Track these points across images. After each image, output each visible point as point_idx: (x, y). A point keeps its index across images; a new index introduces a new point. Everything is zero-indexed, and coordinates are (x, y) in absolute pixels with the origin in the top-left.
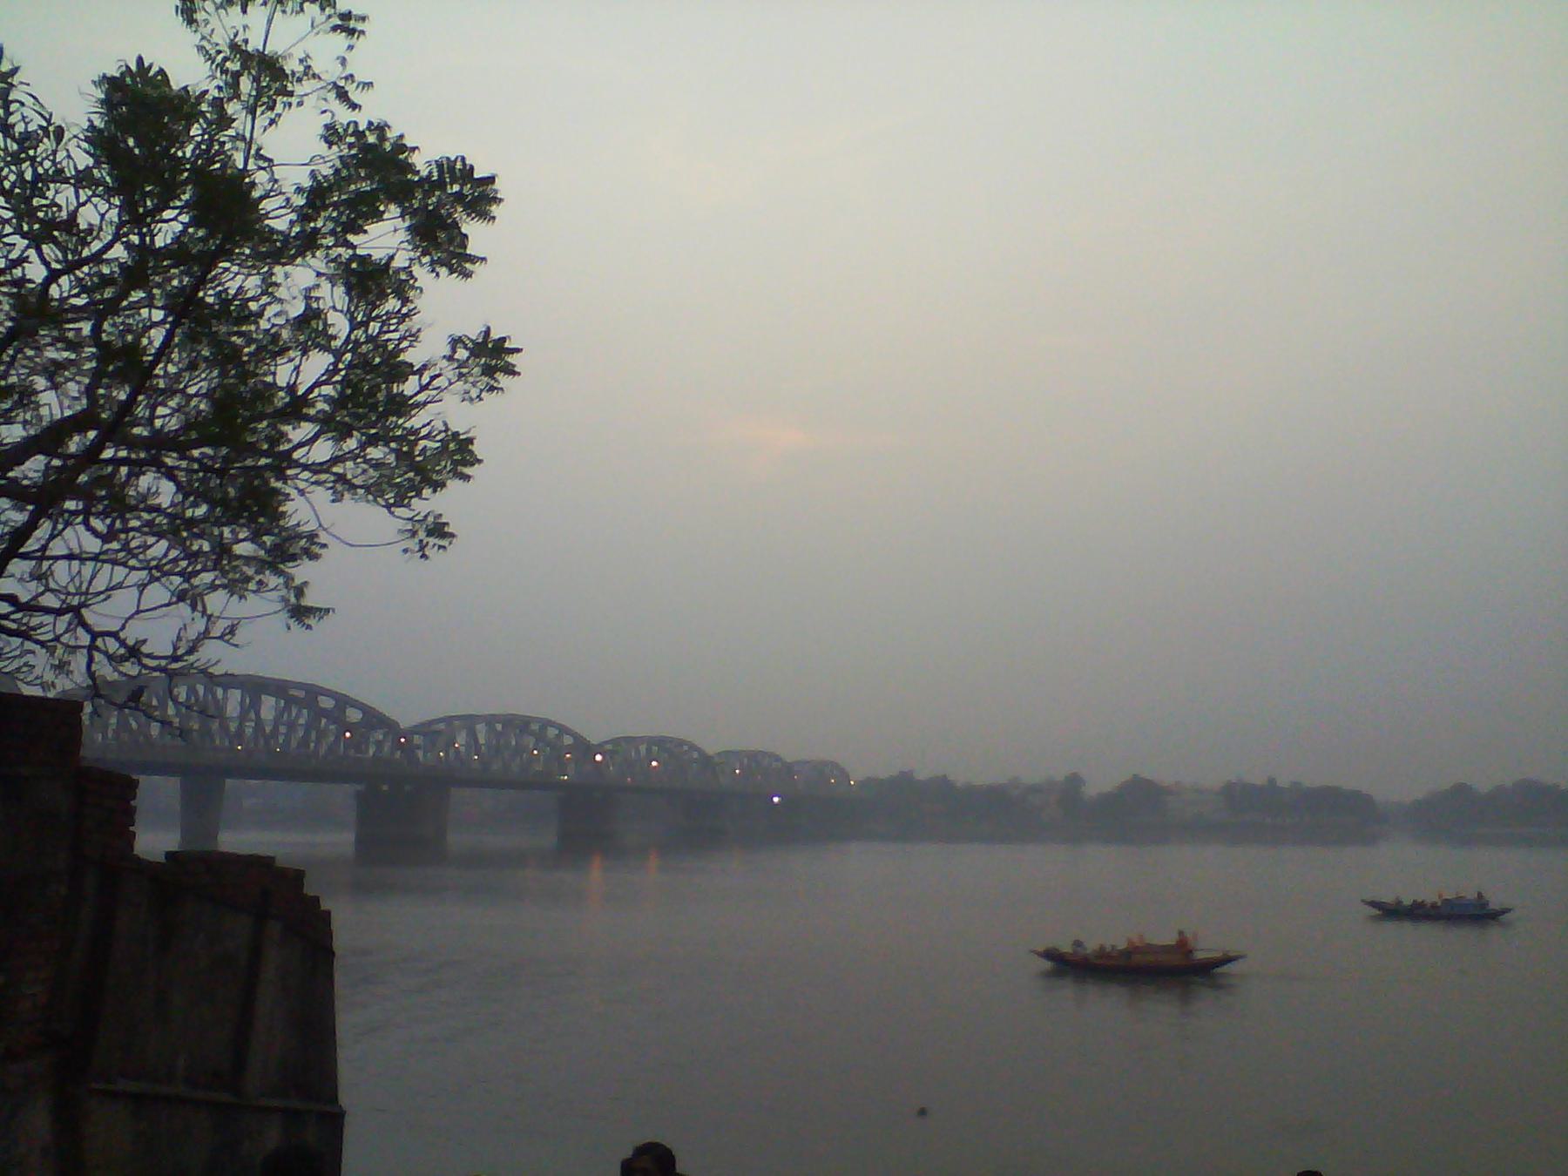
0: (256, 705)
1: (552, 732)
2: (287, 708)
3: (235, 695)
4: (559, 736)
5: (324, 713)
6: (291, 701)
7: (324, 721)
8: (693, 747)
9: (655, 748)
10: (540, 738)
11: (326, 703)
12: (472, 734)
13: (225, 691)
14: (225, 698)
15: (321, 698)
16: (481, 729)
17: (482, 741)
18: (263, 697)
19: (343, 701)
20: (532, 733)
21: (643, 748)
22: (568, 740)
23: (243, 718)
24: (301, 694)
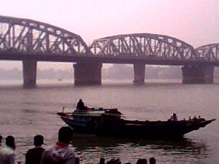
5: (169, 44)
11: (170, 41)
14: (141, 41)
19: (175, 40)
24: (162, 38)
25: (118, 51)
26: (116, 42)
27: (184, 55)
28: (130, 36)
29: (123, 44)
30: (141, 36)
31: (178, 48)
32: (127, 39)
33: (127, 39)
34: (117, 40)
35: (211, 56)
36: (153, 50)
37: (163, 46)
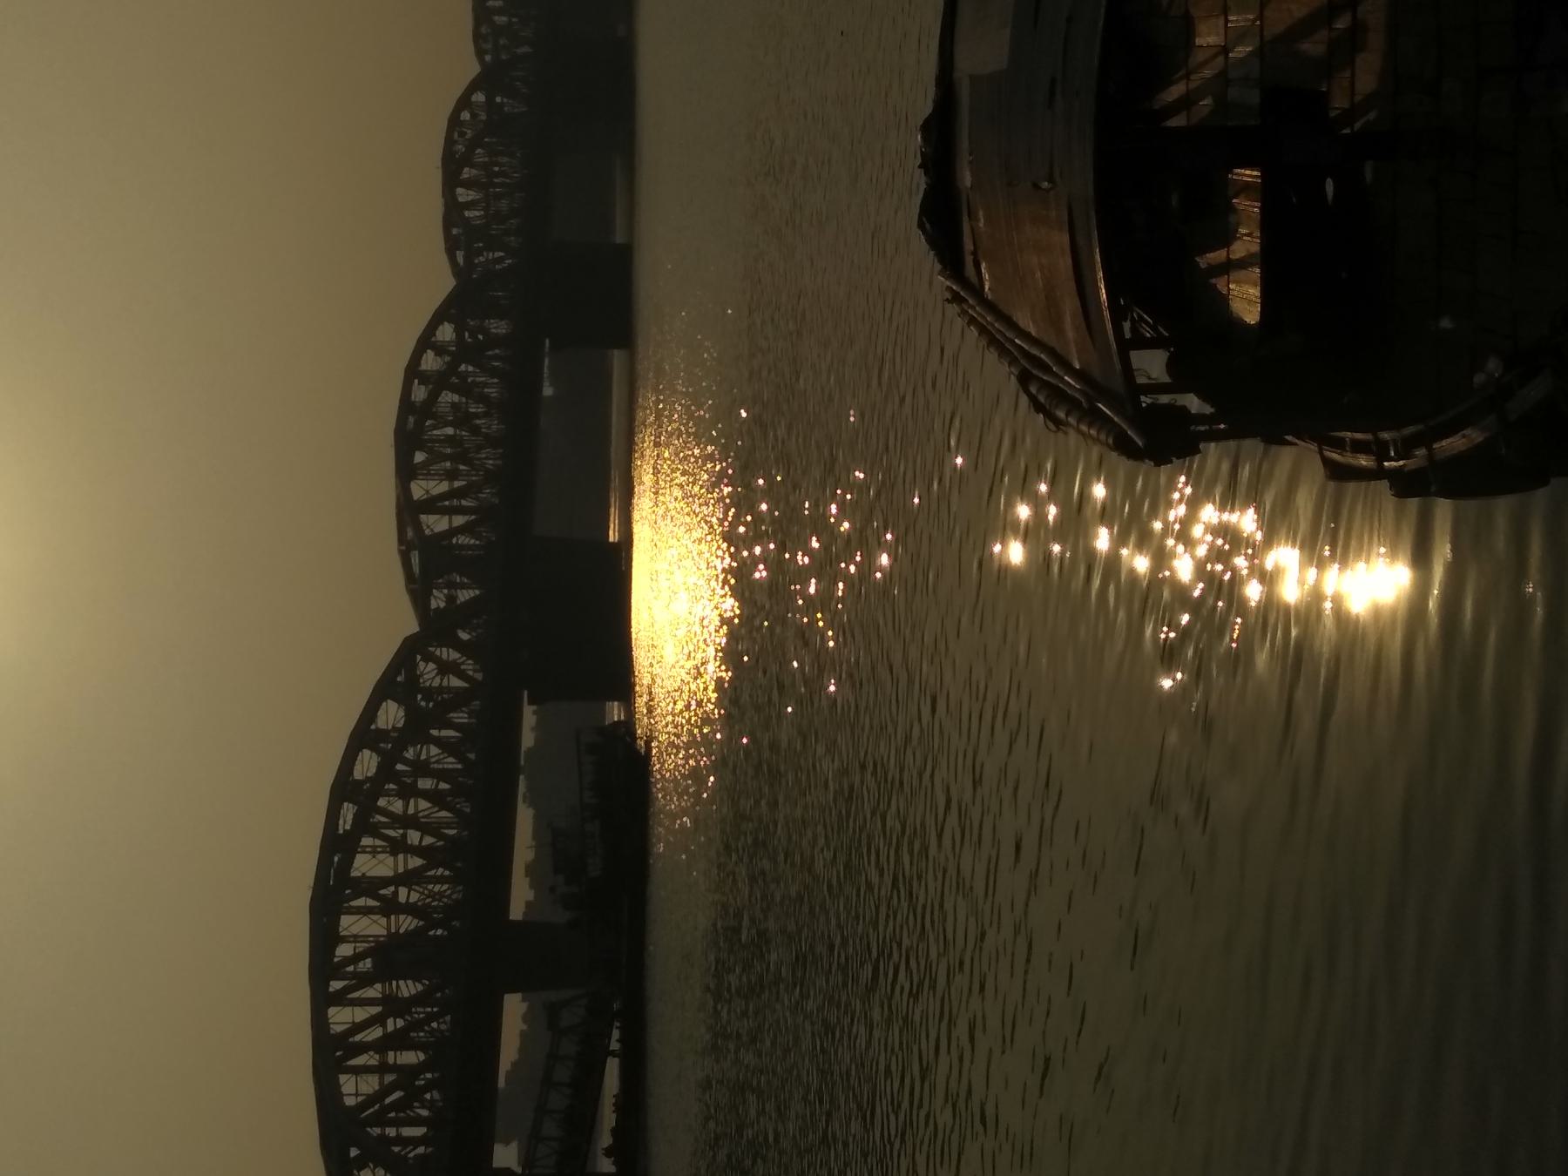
0: (370, 886)
1: (430, 362)
2: (395, 777)
3: (349, 924)
4: (440, 350)
5: (386, 771)
6: (363, 825)
7: (399, 767)
8: (464, 102)
9: (467, 173)
10: (438, 382)
11: (367, 764)
12: (431, 505)
13: (344, 940)
14: (355, 938)
15: (358, 774)
16: (418, 490)
17: (444, 487)
18: (355, 874)
19: (363, 735)
20: (433, 397)
21: (464, 195)
22: (446, 333)
23: (390, 907)
24: (348, 812)
25: (411, 1072)
26: (353, 1089)
27: (456, 682)
28: (322, 1001)
29: (381, 1046)
30: (324, 934)
31: (416, 729)
32: (340, 1018)
33: (340, 1018)
34: (343, 1078)
35: (463, 540)
36: (416, 862)
37: (397, 806)
